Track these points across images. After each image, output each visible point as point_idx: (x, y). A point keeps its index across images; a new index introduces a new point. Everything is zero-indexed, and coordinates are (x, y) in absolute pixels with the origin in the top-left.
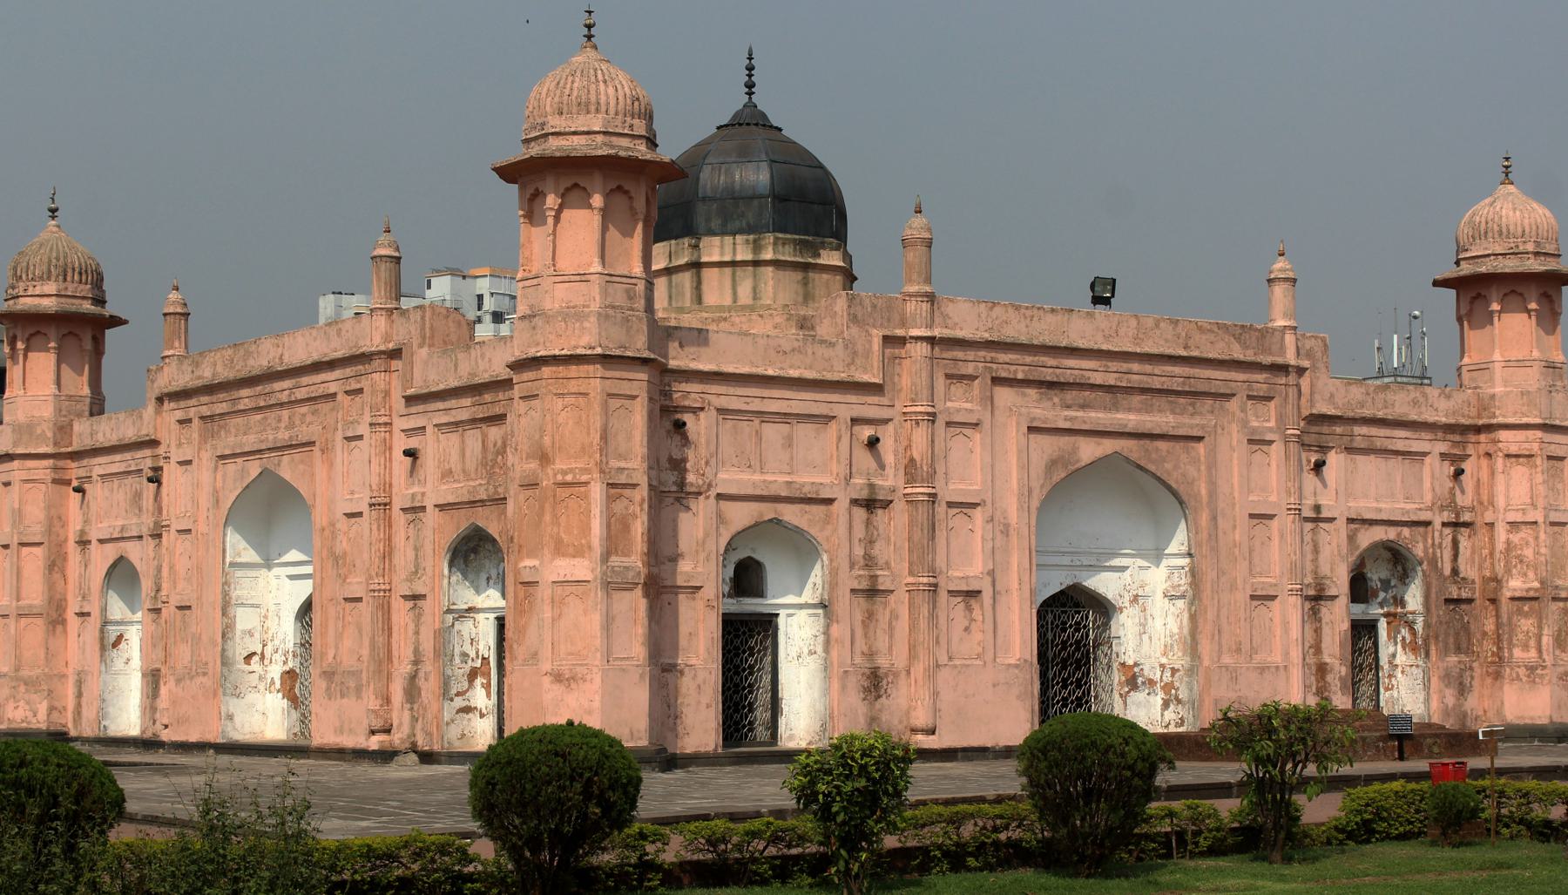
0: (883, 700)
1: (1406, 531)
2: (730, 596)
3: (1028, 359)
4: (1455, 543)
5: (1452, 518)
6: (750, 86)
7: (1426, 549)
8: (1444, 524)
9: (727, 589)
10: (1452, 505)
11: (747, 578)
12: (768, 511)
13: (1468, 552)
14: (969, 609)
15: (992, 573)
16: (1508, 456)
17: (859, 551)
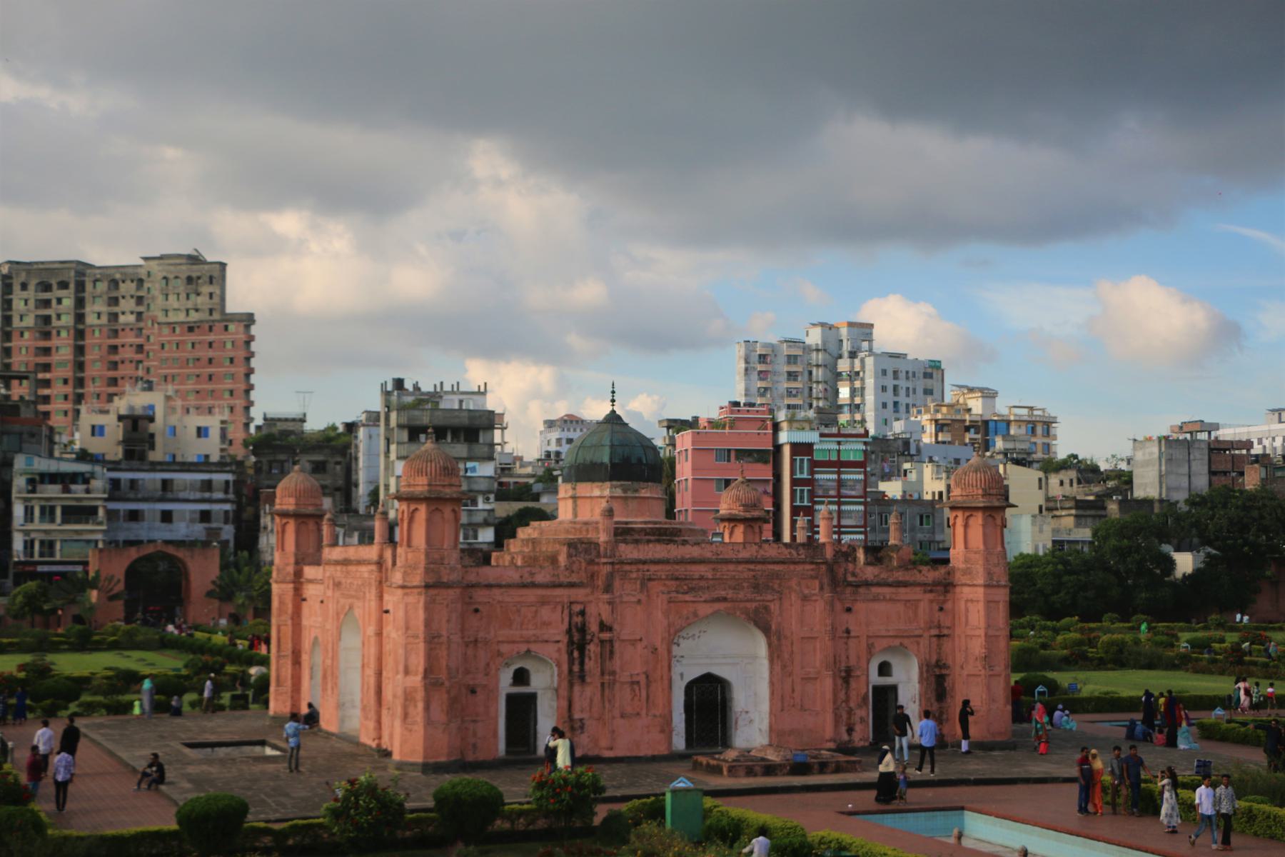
3: (668, 567)
6: (613, 401)
11: (521, 677)
12: (523, 648)
16: (967, 601)
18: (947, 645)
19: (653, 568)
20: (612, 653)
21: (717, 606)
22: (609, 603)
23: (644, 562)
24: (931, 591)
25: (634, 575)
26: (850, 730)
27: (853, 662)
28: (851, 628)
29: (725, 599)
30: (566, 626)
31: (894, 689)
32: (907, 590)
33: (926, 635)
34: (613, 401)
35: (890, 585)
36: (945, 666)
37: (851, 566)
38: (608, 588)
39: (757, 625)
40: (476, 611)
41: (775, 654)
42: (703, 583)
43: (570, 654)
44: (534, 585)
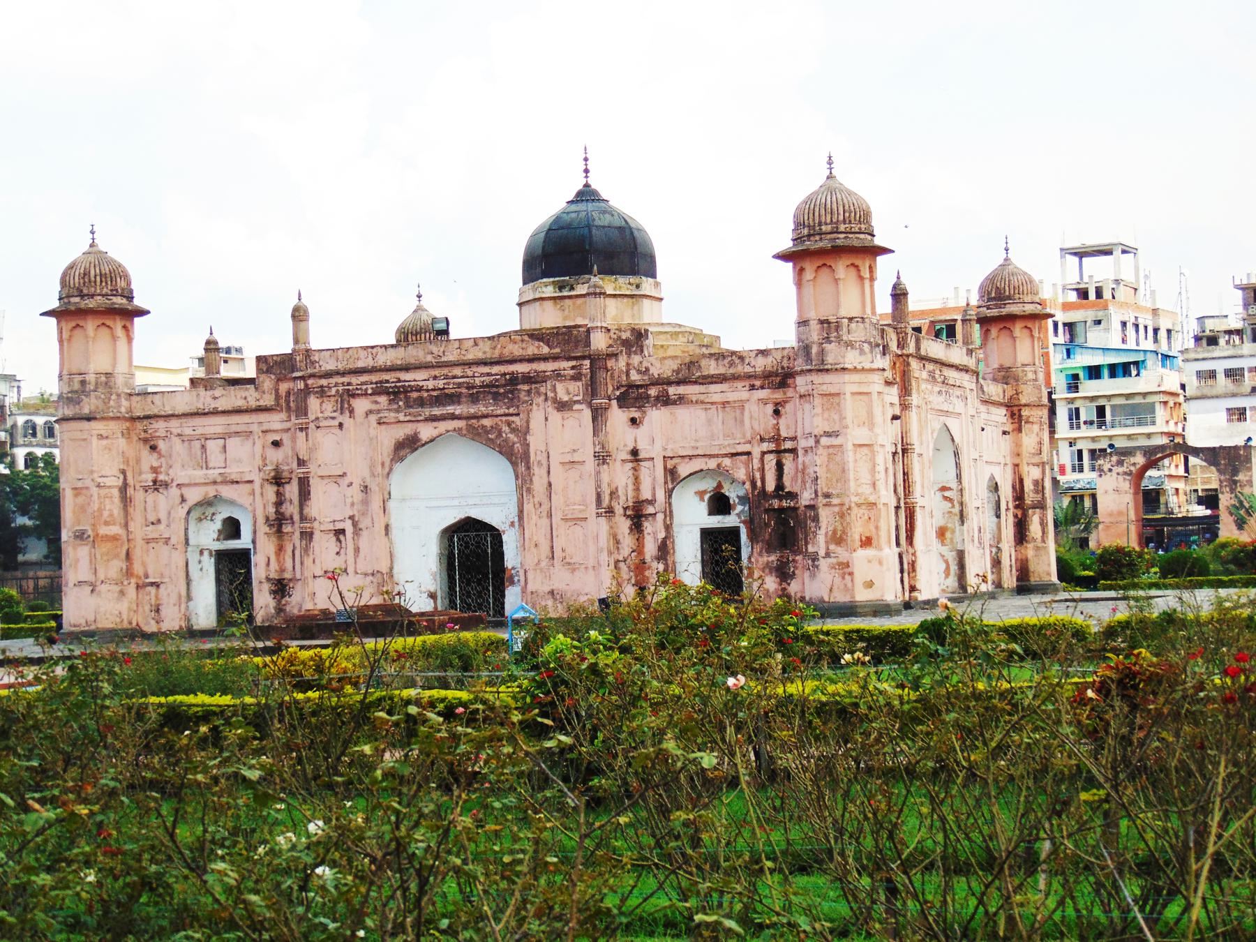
0: (287, 598)
1: (727, 462)
2: (218, 540)
3: (375, 378)
4: (780, 467)
5: (772, 446)
6: (586, 171)
7: (748, 474)
8: (763, 453)
9: (215, 536)
10: (777, 439)
11: (232, 528)
12: (211, 491)
13: (793, 472)
14: (339, 540)
15: (351, 518)
17: (271, 510)
18: (788, 462)
19: (355, 380)
22: (301, 429)
23: (343, 374)
25: (333, 391)
27: (646, 494)
28: (641, 446)
29: (453, 417)
30: (259, 462)
31: (733, 534)
32: (724, 386)
36: (792, 496)
37: (636, 359)
38: (302, 411)
41: (524, 485)
44: (215, 412)
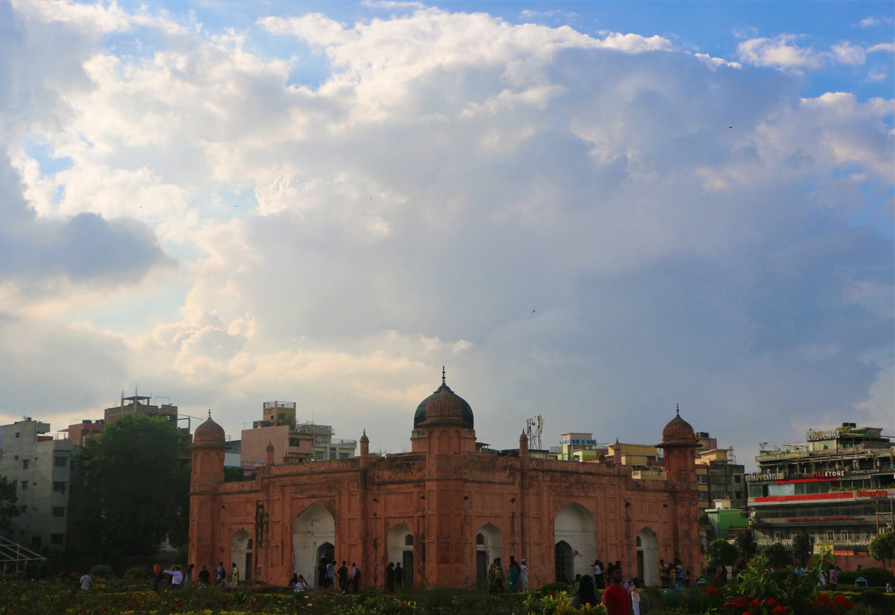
1: (406, 520)
6: (444, 378)
12: (240, 526)
19: (285, 479)
20: (267, 529)
21: (313, 500)
24: (418, 486)
26: (376, 580)
29: (314, 496)
33: (416, 516)
34: (444, 378)
35: (395, 483)
38: (267, 493)
39: (329, 511)
40: (223, 507)
42: (307, 487)
43: (257, 531)
